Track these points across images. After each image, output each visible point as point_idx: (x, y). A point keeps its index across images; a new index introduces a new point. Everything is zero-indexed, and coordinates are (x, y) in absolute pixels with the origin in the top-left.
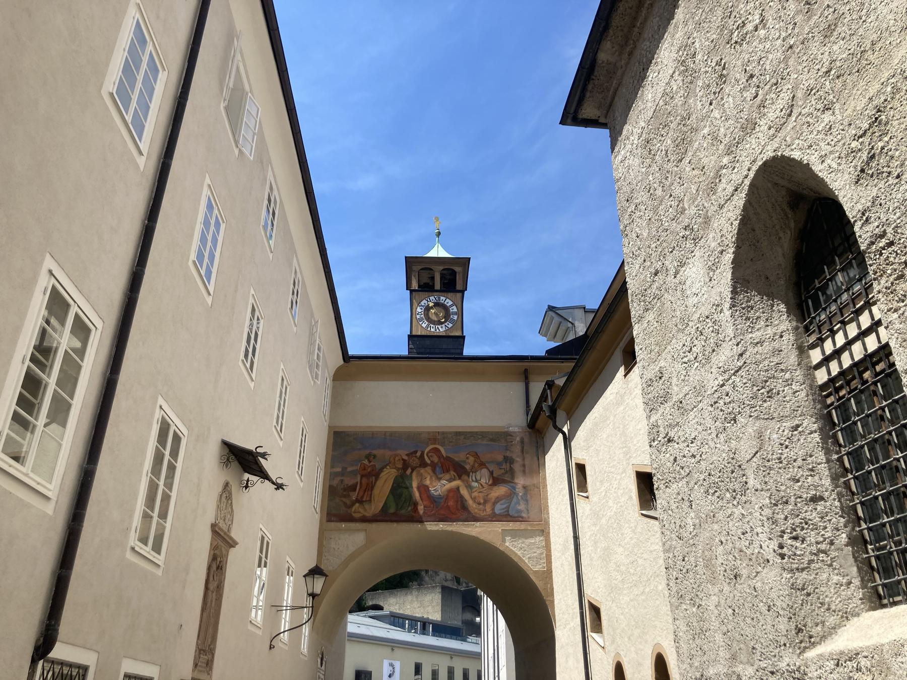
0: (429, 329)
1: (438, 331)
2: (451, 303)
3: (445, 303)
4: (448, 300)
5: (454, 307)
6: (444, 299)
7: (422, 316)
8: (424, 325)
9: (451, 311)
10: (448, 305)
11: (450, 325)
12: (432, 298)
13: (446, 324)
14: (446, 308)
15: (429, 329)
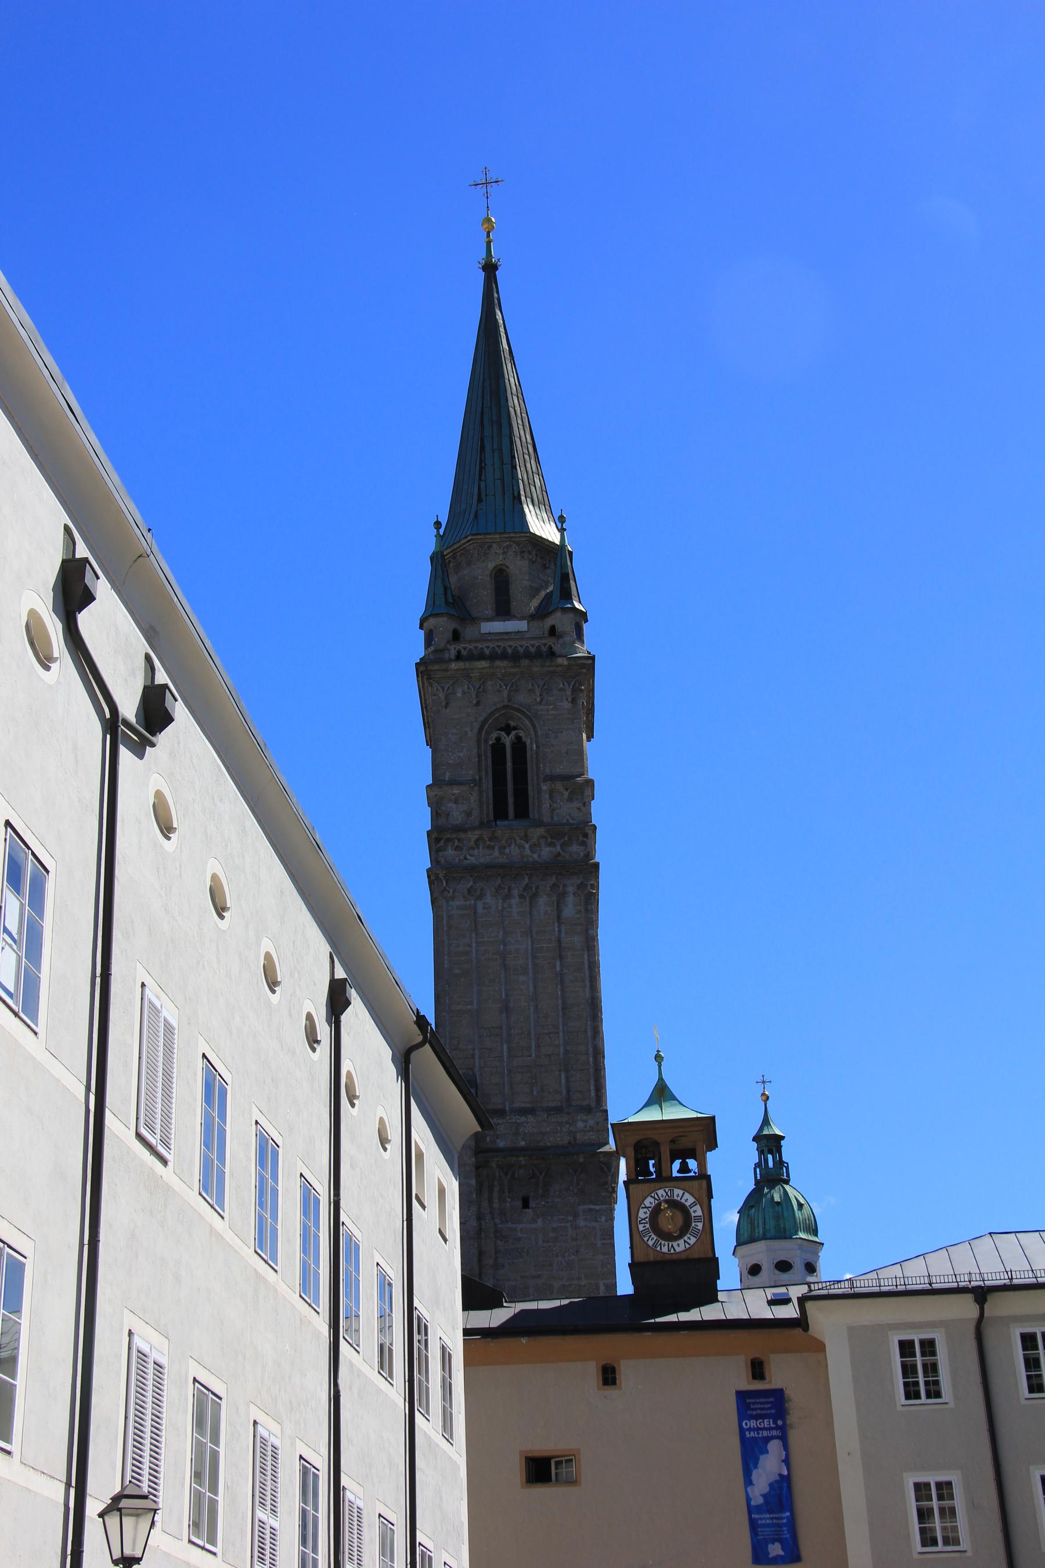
0: (659, 1249)
1: (672, 1251)
2: (691, 1200)
3: (683, 1201)
4: (687, 1195)
5: (698, 1208)
6: (681, 1192)
7: (648, 1226)
8: (650, 1243)
9: (693, 1214)
10: (688, 1204)
11: (693, 1240)
12: (661, 1192)
13: (686, 1238)
14: (684, 1210)
15: (659, 1249)
